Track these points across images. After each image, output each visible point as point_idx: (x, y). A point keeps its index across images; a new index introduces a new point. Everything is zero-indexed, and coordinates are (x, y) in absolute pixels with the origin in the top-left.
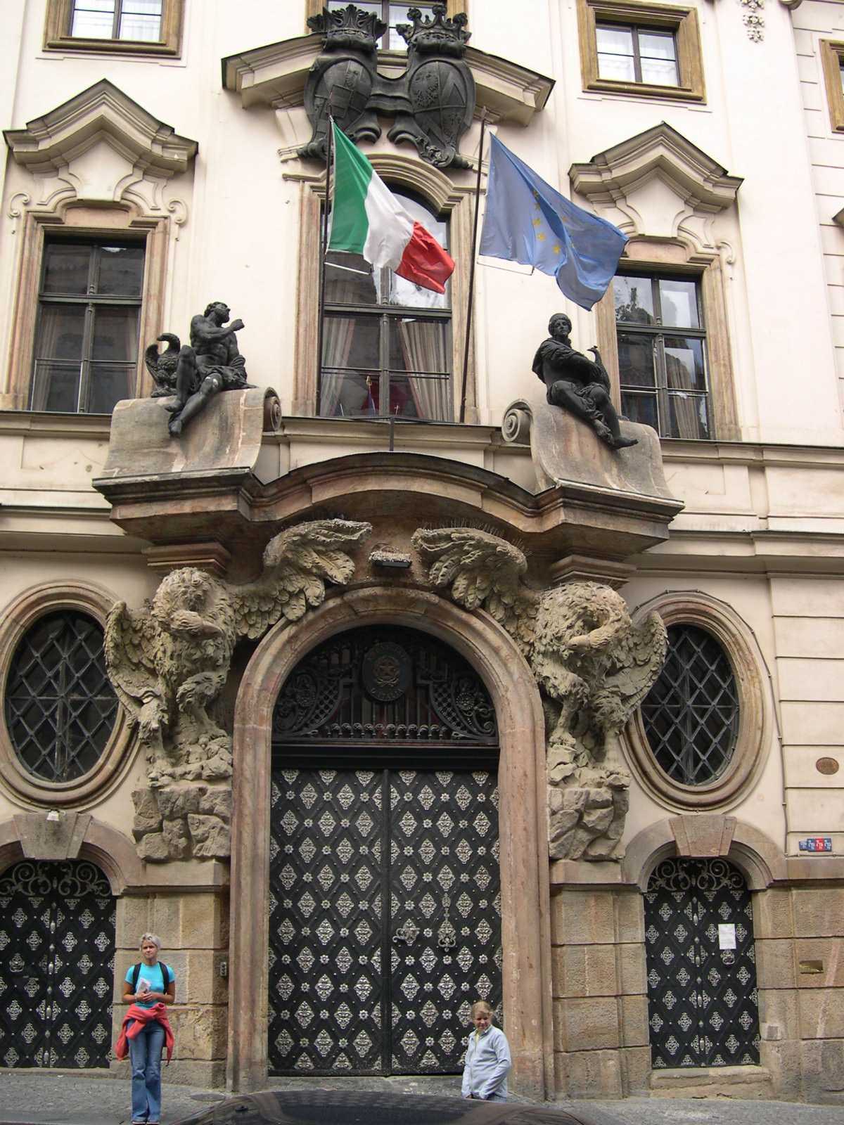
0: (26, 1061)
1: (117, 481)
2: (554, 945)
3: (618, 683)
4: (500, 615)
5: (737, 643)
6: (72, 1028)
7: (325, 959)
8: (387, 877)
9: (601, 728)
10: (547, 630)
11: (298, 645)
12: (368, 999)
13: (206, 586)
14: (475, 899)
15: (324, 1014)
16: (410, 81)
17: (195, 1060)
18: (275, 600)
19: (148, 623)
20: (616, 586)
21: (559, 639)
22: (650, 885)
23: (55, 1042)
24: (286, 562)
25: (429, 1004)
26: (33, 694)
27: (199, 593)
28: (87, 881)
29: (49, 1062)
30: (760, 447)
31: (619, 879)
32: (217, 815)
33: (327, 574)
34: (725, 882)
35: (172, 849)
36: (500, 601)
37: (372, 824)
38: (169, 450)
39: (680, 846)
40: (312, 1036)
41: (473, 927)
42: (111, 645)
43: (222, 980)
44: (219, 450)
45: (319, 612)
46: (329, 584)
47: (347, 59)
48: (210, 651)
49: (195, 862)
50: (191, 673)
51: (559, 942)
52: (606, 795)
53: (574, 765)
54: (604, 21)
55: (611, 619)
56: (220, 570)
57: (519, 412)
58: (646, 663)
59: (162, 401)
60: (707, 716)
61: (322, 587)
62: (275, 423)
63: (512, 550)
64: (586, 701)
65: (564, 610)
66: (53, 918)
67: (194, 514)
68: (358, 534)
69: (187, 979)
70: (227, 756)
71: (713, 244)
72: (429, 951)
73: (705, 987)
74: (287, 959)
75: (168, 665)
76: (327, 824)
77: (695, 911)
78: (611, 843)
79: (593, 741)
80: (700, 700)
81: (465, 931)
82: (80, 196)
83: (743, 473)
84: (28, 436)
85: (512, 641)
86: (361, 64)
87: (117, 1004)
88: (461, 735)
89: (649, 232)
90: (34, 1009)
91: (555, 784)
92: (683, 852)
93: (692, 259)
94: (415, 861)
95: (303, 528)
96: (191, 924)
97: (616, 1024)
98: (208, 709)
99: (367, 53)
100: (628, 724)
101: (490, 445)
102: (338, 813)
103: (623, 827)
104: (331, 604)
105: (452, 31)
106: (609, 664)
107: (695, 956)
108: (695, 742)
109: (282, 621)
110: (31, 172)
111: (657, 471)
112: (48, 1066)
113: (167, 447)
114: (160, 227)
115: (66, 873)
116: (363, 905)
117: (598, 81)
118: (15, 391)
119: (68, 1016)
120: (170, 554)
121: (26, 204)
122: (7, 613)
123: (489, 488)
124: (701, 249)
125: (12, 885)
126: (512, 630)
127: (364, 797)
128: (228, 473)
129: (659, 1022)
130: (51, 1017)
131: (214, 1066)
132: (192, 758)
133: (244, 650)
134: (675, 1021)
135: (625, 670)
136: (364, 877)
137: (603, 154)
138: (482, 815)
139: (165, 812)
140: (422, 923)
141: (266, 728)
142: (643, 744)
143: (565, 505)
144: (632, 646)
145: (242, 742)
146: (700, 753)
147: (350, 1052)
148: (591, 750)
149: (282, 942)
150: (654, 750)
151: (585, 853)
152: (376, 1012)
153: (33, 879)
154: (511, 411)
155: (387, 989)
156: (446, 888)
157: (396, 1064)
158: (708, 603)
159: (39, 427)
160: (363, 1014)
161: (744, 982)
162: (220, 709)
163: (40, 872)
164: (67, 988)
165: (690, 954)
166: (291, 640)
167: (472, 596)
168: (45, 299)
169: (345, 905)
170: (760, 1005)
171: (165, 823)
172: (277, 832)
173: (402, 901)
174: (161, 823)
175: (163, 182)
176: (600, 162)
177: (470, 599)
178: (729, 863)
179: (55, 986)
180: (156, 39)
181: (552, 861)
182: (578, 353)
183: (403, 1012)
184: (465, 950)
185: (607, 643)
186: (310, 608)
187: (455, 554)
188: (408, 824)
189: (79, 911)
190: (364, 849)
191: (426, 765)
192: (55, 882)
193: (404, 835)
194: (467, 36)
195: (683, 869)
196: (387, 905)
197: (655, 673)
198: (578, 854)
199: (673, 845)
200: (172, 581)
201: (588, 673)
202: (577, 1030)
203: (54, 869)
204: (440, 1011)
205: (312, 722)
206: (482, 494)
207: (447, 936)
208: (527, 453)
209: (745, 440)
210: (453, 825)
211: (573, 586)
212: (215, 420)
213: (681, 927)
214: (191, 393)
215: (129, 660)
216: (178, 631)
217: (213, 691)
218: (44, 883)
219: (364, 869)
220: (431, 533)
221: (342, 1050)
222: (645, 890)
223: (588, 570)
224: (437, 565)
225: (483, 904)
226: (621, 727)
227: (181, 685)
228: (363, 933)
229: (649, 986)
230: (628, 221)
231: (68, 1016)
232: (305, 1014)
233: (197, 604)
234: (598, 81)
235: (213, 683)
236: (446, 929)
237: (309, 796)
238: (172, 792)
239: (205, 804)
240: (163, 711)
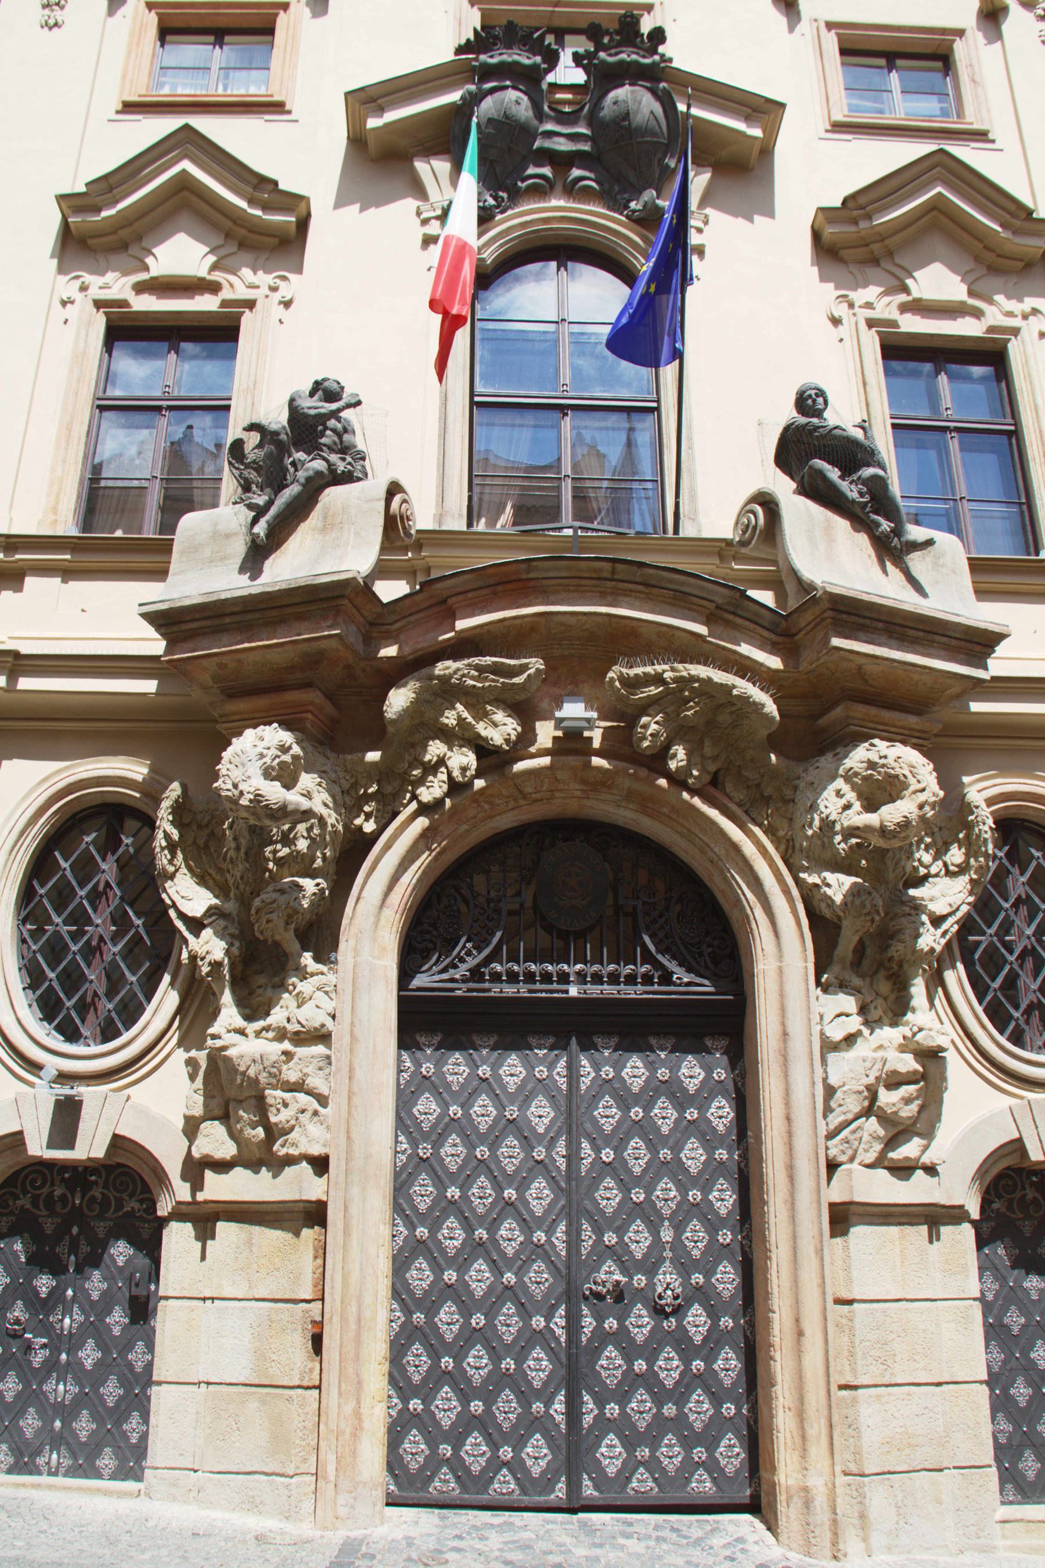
4: (740, 795)
7: (478, 1320)
9: (900, 965)
12: (546, 1383)
25: (641, 1394)
26: (57, 920)
28: (125, 1196)
29: (57, 1469)
32: (309, 1093)
37: (552, 1114)
40: (458, 1441)
68: (525, 676)
88: (686, 980)
94: (617, 1169)
109: (414, 805)
115: (96, 1183)
123: (717, 607)
147: (516, 1466)
148: (885, 999)
150: (980, 1003)
153: (45, 1190)
154: (748, 508)
155: (574, 1371)
156: (666, 1212)
157: (588, 1490)
163: (57, 1179)
164: (89, 1355)
169: (510, 1235)
172: (404, 1122)
192: (78, 1195)
193: (600, 1129)
195: (1032, 1184)
198: (871, 1157)
199: (1017, 1146)
205: (462, 960)
218: (63, 1198)
221: (505, 1464)
224: (644, 720)
227: (258, 895)
240: (232, 936)
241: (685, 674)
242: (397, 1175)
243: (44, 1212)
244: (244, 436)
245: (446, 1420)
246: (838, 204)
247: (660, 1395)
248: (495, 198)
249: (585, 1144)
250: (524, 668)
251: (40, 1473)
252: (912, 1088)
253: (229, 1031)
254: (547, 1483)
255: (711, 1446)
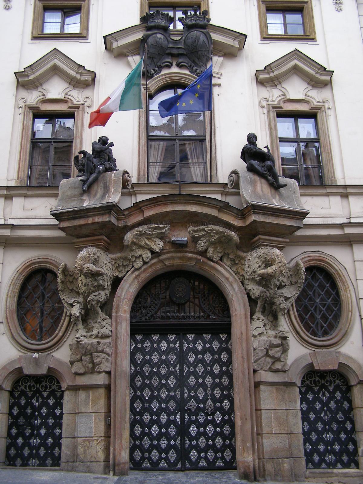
0: (25, 464)
1: (60, 211)
2: (257, 410)
3: (283, 292)
4: (229, 263)
5: (338, 273)
6: (45, 449)
8: (182, 381)
9: (276, 312)
10: (249, 269)
11: (140, 279)
12: (175, 435)
13: (98, 254)
14: (222, 390)
15: (155, 442)
16: (184, 40)
17: (97, 462)
18: (130, 260)
19: (76, 272)
20: (280, 249)
21: (255, 272)
22: (302, 384)
23: (37, 455)
24: (133, 243)
27: (96, 257)
30: (346, 187)
31: (287, 380)
32: (105, 353)
33: (151, 248)
34: (337, 382)
35: (86, 369)
36: (228, 257)
37: (175, 357)
38: (82, 198)
39: (315, 365)
41: (221, 403)
42: (60, 282)
43: (108, 426)
44: (103, 197)
45: (149, 264)
46: (153, 252)
47: (156, 33)
48: (101, 282)
49: (96, 373)
50: (93, 292)
51: (259, 408)
52: (278, 341)
53: (264, 328)
54: (270, 10)
55: (277, 262)
56: (105, 247)
57: (234, 175)
58: (296, 283)
59: (80, 178)
60: (326, 307)
61: (150, 254)
62: (128, 185)
63: (233, 234)
64: (268, 299)
65: (257, 260)
66: (37, 401)
67: (93, 223)
69: (93, 426)
70: (109, 328)
71: (321, 101)
72: (201, 413)
73: (331, 430)
74: (138, 417)
75: (83, 289)
76: (155, 358)
77: (324, 395)
78: (282, 363)
79: (273, 318)
80: (322, 300)
81: (218, 405)
82: (47, 98)
83: (338, 199)
84: (26, 196)
85: (234, 275)
86: (163, 35)
87: (64, 438)
89: (292, 97)
90: (29, 441)
91: (255, 337)
92: (316, 368)
93: (312, 108)
94: (195, 373)
95: (140, 228)
96: (95, 402)
97: (288, 447)
98: (102, 308)
99: (165, 29)
100: (289, 311)
101: (223, 191)
102: (160, 353)
103: (287, 356)
104: (154, 261)
105: (202, 18)
106: (278, 284)
107: (325, 416)
108: (321, 318)
109: (133, 269)
110: (27, 89)
111: (297, 198)
112: (34, 466)
113: (82, 196)
114: (81, 108)
116: (172, 393)
117: (267, 35)
118: (21, 178)
119: (43, 444)
120: (84, 241)
121: (25, 102)
122: (17, 270)
124: (316, 103)
125: (20, 386)
126: (235, 270)
127: (172, 346)
128: (106, 205)
129: (309, 447)
130: (36, 444)
131: (104, 465)
132: (94, 329)
133: (116, 282)
134: (317, 447)
135: (286, 287)
136: (172, 381)
137: (269, 65)
138: (224, 353)
139: (82, 352)
140: (198, 401)
141: (128, 315)
142: (296, 319)
143: (254, 213)
144: (289, 275)
145: (116, 321)
146: (323, 323)
147: (167, 459)
148: (272, 322)
149: (136, 410)
150: (302, 323)
151: (270, 368)
152: (178, 441)
153: (28, 384)
155: (183, 431)
157: (187, 465)
158: (324, 256)
159: (31, 192)
160: (173, 442)
161: (349, 429)
162: (107, 306)
164: (43, 431)
165: (322, 415)
166: (136, 277)
167: (216, 255)
168: (34, 141)
169: (164, 393)
170: (357, 439)
171: (83, 357)
172: (133, 361)
173: (189, 392)
174: (81, 357)
175: (81, 90)
176: (268, 68)
177: (215, 256)
178: (338, 373)
179: (38, 430)
180: (78, 32)
181: (255, 371)
182: (259, 149)
183: (191, 441)
184: (218, 413)
185: (275, 272)
186: (145, 263)
187: (207, 237)
188: (191, 357)
189: (48, 397)
190: (172, 369)
191: (199, 330)
192: (38, 385)
193: (189, 362)
194: (209, 20)
195: (318, 376)
196: (182, 394)
197: (300, 287)
198: (268, 368)
199: (311, 365)
200: (84, 253)
201: (269, 287)
202: (269, 449)
203: (37, 379)
204: (207, 441)
206: (219, 211)
207: (210, 406)
208: (238, 194)
209: (338, 184)
210: (211, 357)
211: (260, 249)
212: (102, 184)
213: (317, 403)
214: (91, 174)
215: (68, 288)
216: (86, 273)
217: (103, 299)
218: (34, 386)
219: (172, 377)
220: (196, 228)
221: (163, 458)
222: (300, 385)
223: (267, 242)
224: (200, 242)
225: (226, 392)
226: (284, 311)
228: (172, 405)
229: (303, 429)
230: (282, 93)
231: (43, 444)
232: (146, 442)
233: (95, 262)
234: (267, 35)
235: (103, 296)
236: (209, 403)
237: (147, 346)
238: (85, 343)
239: (100, 349)
241: (211, 228)
242: (131, 376)
243: (28, 390)
244: (78, 154)
245: (146, 446)
246: (263, 69)
247: (208, 438)
248: (154, 70)
249: (185, 366)
250: (164, 228)
251: (29, 466)
252: (278, 349)
253: (82, 336)
254: (175, 464)
255: (223, 453)
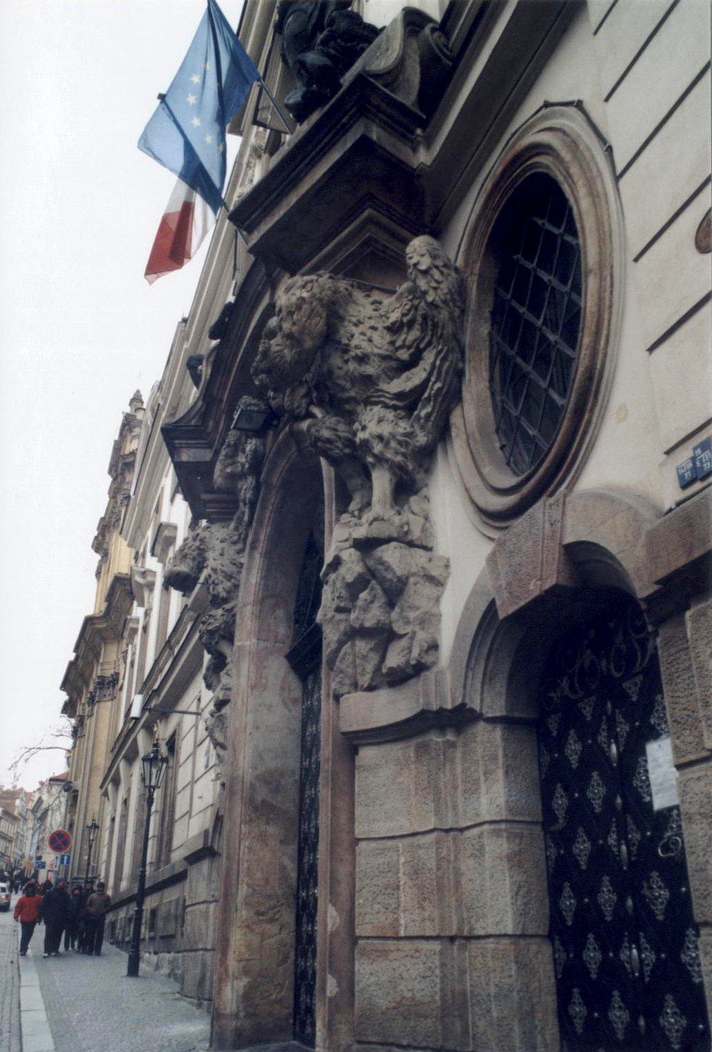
78: (403, 643)
107: (618, 841)
